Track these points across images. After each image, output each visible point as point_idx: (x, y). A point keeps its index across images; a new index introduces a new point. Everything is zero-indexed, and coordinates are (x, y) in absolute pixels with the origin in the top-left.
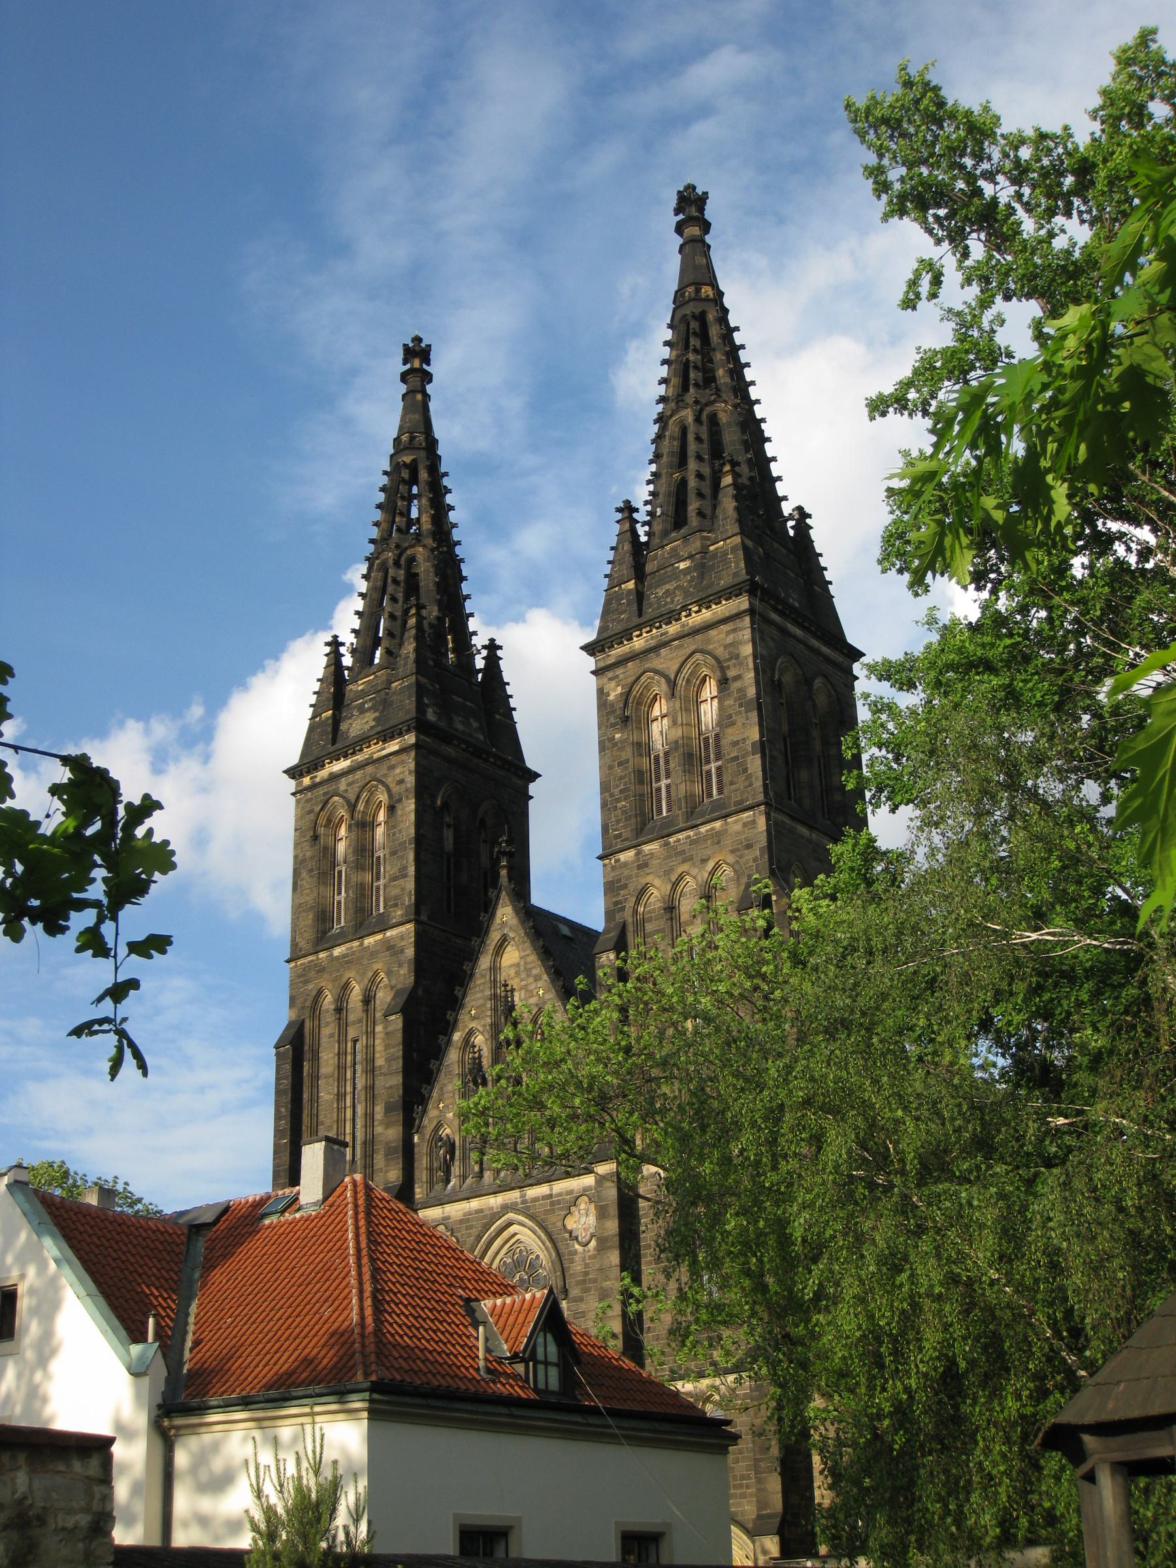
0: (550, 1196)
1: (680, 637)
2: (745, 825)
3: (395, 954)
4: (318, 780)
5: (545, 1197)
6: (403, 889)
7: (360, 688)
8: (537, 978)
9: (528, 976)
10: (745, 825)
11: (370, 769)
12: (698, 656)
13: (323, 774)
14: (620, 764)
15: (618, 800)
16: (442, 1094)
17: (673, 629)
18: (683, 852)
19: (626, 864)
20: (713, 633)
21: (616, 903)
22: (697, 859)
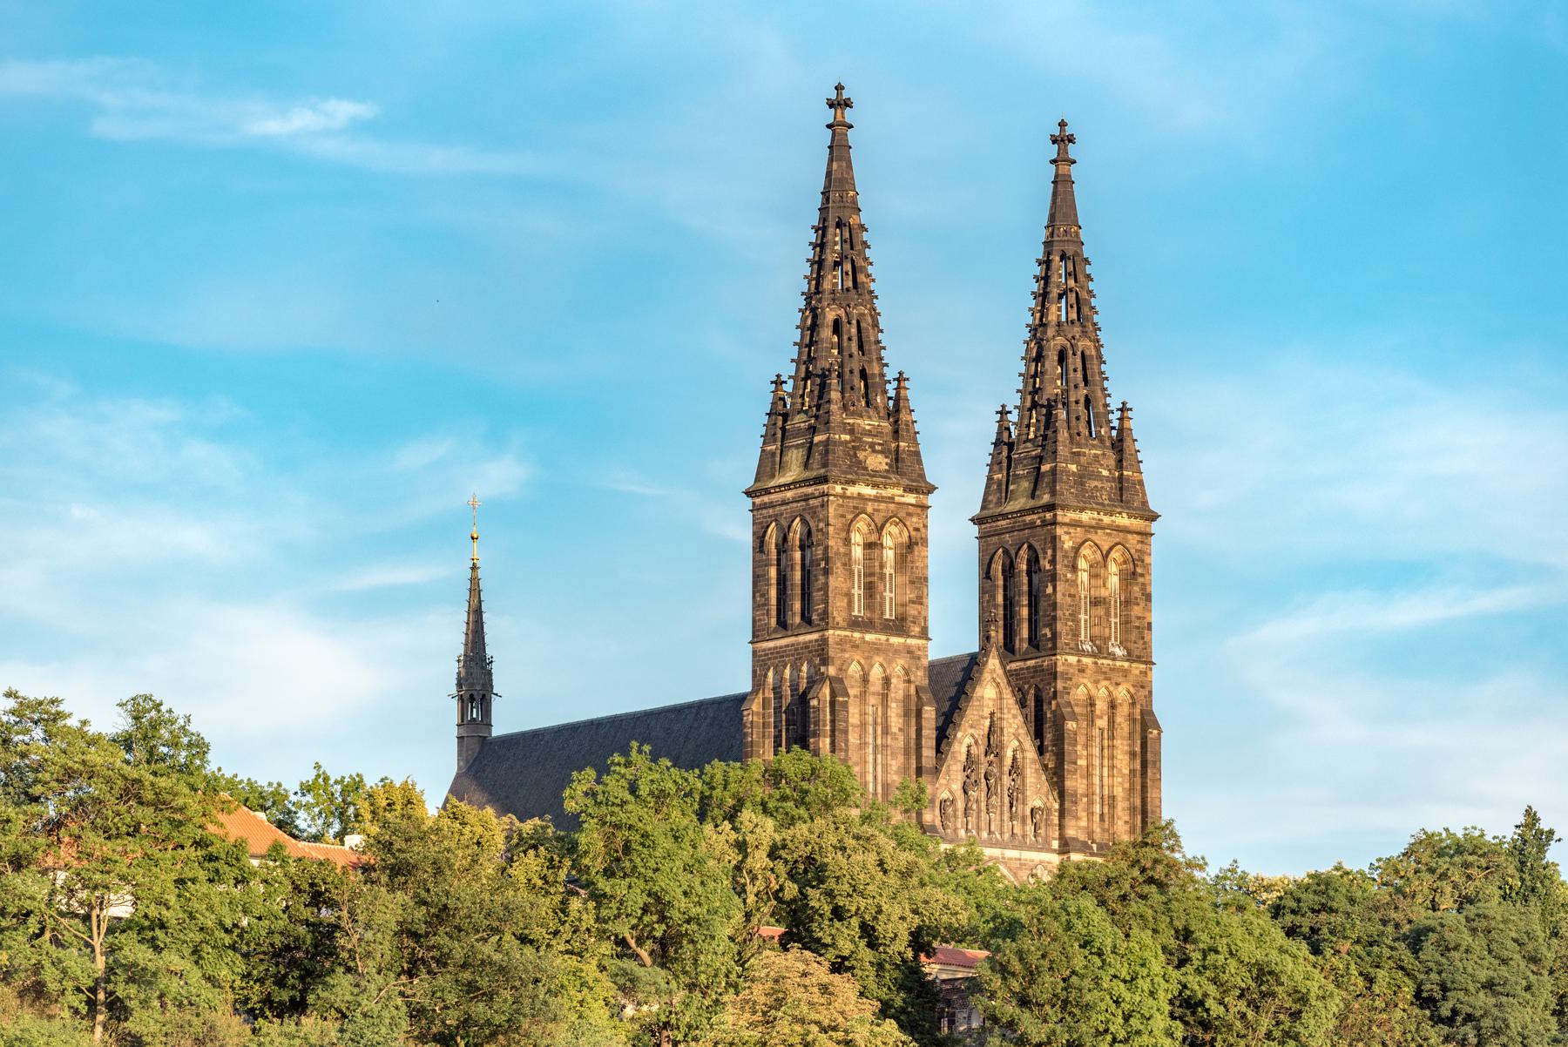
0: (1020, 859)
1: (1109, 527)
2: (1141, 672)
3: (913, 658)
4: (848, 493)
5: (1016, 859)
6: (919, 613)
7: (868, 427)
8: (1014, 717)
9: (1009, 712)
10: (1141, 672)
11: (892, 506)
12: (1120, 546)
13: (853, 490)
14: (1070, 596)
15: (1068, 620)
16: (948, 771)
17: (1107, 520)
18: (1105, 673)
19: (1070, 665)
20: (1130, 536)
21: (1065, 688)
22: (1113, 682)
